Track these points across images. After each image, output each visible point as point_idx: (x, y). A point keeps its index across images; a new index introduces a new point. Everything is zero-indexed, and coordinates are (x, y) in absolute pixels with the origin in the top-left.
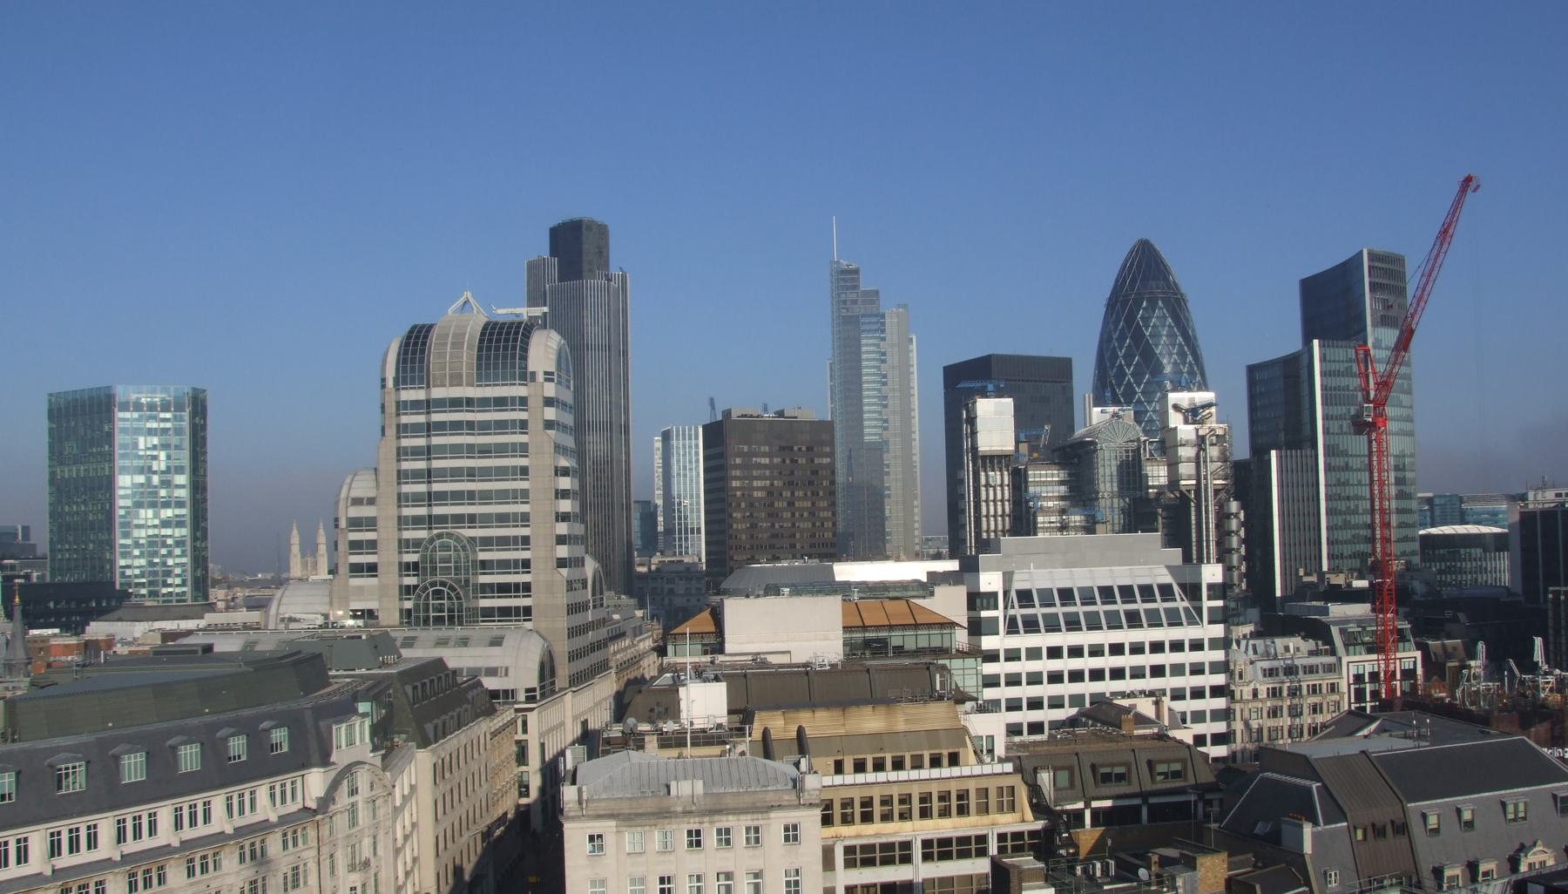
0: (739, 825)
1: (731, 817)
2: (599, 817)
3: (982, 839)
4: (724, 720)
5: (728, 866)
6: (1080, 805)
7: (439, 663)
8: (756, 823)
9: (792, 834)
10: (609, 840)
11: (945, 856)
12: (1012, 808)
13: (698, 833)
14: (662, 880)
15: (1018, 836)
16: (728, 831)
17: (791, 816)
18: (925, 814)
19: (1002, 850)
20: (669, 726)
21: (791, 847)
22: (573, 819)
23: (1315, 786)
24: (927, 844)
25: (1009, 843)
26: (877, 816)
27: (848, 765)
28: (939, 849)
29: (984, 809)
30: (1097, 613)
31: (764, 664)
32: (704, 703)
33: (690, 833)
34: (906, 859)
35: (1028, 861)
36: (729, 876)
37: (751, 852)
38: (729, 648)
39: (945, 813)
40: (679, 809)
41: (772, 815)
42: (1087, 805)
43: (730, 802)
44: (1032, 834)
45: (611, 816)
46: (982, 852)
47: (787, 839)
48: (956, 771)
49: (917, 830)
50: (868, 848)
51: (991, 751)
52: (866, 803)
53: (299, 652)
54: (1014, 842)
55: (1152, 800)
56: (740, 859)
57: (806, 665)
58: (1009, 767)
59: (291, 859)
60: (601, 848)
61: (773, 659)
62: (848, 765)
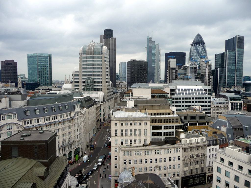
0: (138, 122)
1: (137, 121)
2: (117, 120)
3: (173, 126)
4: (134, 107)
6: (188, 122)
7: (89, 96)
8: (140, 122)
9: (146, 124)
10: (118, 124)
11: (167, 129)
13: (132, 123)
15: (178, 126)
16: (136, 123)
17: (146, 122)
18: (164, 122)
19: (176, 128)
20: (126, 107)
21: (145, 126)
22: (112, 121)
23: (227, 121)
24: (164, 127)
25: (177, 127)
26: (157, 122)
27: (153, 114)
28: (166, 128)
29: (173, 122)
30: (200, 93)
31: (139, 98)
32: (131, 104)
33: (130, 123)
34: (161, 129)
35: (181, 130)
36: (136, 130)
37: (140, 127)
38: (134, 96)
39: (167, 122)
40: (129, 120)
41: (143, 121)
42: (189, 122)
43: (137, 119)
44: (181, 126)
45: (119, 120)
46: (173, 128)
47: (145, 125)
48: (169, 116)
49: (163, 125)
50: (155, 127)
51: (174, 113)
52: (161, 120)
53: (69, 94)
54: (178, 127)
55: (199, 122)
56: (137, 127)
57: (146, 99)
58: (178, 116)
59: (69, 125)
60: (117, 125)
61: (140, 98)
62: (153, 114)
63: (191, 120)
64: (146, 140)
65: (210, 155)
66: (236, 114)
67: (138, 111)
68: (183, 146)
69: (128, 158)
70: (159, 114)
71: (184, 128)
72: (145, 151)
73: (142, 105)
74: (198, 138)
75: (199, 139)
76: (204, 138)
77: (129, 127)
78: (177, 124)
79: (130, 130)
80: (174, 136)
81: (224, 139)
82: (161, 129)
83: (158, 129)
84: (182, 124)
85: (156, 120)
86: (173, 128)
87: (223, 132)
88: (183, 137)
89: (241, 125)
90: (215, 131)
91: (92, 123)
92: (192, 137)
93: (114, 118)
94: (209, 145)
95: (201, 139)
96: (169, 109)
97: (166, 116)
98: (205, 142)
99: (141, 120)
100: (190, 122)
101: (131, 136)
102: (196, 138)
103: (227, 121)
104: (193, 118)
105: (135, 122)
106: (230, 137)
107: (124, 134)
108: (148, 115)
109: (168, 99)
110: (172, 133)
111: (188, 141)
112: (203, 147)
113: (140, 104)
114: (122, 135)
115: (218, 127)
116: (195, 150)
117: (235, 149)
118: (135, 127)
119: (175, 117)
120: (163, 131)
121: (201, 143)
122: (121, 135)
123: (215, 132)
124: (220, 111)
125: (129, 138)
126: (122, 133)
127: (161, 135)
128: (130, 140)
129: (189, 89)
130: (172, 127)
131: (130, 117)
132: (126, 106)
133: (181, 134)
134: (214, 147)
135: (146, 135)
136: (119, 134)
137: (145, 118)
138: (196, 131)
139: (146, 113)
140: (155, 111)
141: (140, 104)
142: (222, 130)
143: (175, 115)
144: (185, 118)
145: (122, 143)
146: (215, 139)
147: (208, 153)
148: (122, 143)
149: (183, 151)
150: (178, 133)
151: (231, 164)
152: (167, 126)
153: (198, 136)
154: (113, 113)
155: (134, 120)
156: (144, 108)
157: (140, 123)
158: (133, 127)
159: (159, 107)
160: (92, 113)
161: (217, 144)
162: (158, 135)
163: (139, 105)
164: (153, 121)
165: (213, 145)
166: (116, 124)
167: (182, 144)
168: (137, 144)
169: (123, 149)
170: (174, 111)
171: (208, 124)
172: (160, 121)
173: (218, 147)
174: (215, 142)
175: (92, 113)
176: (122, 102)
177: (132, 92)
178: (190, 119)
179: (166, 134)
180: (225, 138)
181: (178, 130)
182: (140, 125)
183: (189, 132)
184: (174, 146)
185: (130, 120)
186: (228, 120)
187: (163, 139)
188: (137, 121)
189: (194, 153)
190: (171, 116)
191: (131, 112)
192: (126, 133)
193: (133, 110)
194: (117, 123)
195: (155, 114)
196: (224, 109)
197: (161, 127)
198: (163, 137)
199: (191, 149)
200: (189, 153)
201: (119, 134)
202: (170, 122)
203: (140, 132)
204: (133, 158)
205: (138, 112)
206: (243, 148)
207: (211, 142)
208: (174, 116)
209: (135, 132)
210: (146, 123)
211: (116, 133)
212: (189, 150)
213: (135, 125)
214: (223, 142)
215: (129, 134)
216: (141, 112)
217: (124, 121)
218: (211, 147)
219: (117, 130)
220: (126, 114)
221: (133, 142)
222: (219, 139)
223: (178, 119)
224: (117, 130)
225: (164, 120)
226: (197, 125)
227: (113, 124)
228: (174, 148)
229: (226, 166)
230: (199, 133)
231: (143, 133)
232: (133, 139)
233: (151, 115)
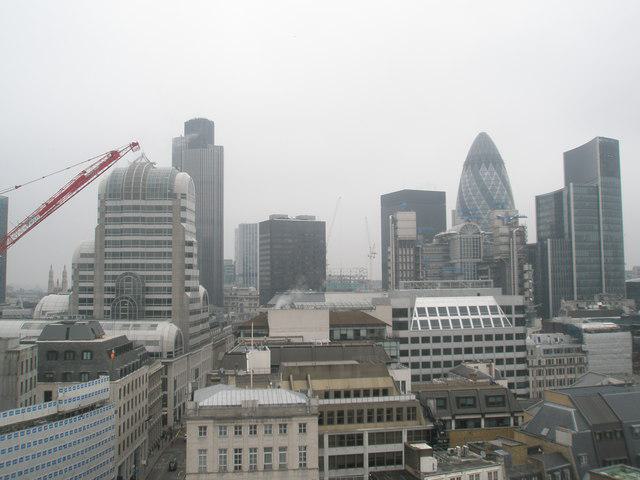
0: (276, 424)
9: (303, 429)
10: (210, 429)
12: (414, 418)
14: (236, 451)
17: (303, 420)
18: (370, 420)
20: (241, 373)
22: (188, 419)
26: (346, 420)
27: (332, 394)
29: (399, 419)
31: (289, 342)
32: (259, 360)
34: (360, 443)
35: (425, 446)
38: (271, 334)
40: (246, 415)
41: (294, 419)
42: (453, 417)
43: (273, 412)
45: (211, 418)
47: (300, 431)
48: (386, 399)
49: (365, 429)
50: (342, 437)
51: (404, 388)
54: (415, 436)
56: (276, 440)
57: (311, 343)
60: (205, 434)
62: (332, 394)
66: (602, 386)
67: (277, 384)
70: (342, 394)
71: (436, 438)
73: (291, 364)
74: (479, 471)
77: (246, 441)
78: (413, 426)
82: (360, 443)
84: (430, 426)
85: (331, 414)
87: (560, 449)
88: (430, 470)
90: (537, 444)
91: (132, 429)
92: (461, 466)
95: (490, 474)
97: (376, 399)
100: (457, 417)
103: (572, 411)
105: (269, 422)
106: (584, 462)
107: (231, 465)
110: (394, 458)
115: (545, 432)
118: (266, 438)
119: (405, 402)
123: (536, 448)
126: (223, 460)
127: (361, 465)
129: (424, 309)
130: (394, 437)
132: (245, 368)
133: (422, 458)
135: (305, 465)
138: (472, 448)
139: (306, 392)
140: (338, 384)
141: (290, 359)
142: (558, 440)
143: (408, 397)
144: (443, 403)
150: (413, 457)
156: (302, 374)
157: (285, 426)
158: (261, 441)
159: (353, 372)
160: (131, 396)
162: (351, 466)
163: (286, 364)
164: (325, 417)
166: (203, 430)
170: (404, 382)
171: (516, 424)
175: (131, 396)
176: (233, 354)
177: (266, 317)
179: (376, 459)
181: (413, 446)
185: (251, 417)
186: (576, 407)
188: (273, 417)
190: (391, 398)
191: (254, 387)
193: (261, 381)
194: (205, 428)
195: (337, 395)
196: (561, 372)
197: (360, 436)
202: (389, 419)
203: (283, 457)
205: (279, 387)
208: (402, 398)
209: (268, 458)
210: (305, 425)
211: (203, 460)
216: (291, 389)
219: (205, 451)
220: (238, 396)
222: (548, 472)
223: (414, 409)
224: (205, 451)
225: (370, 412)
226: (480, 426)
227: (192, 430)
230: (483, 454)
231: (293, 461)
233: (327, 395)
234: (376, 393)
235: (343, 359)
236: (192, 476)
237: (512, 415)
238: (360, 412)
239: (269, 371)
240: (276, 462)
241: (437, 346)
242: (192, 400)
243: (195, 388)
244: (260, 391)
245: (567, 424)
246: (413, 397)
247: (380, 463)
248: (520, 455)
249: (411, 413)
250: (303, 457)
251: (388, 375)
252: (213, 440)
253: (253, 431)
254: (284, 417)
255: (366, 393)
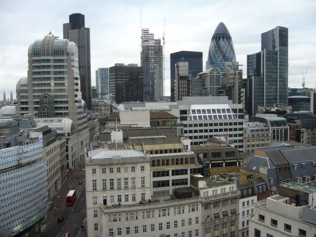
2: (95, 165)
3: (186, 170)
5: (126, 177)
9: (143, 169)
10: (98, 170)
11: (177, 174)
12: (194, 163)
17: (143, 165)
20: (109, 142)
22: (87, 166)
24: (173, 171)
27: (154, 152)
28: (175, 173)
29: (186, 163)
31: (130, 127)
32: (117, 136)
33: (117, 168)
34: (168, 175)
36: (127, 179)
37: (133, 173)
38: (121, 123)
39: (177, 164)
42: (210, 162)
43: (128, 161)
44: (199, 169)
46: (186, 173)
47: (141, 170)
48: (180, 154)
49: (170, 168)
51: (187, 149)
53: (12, 124)
54: (194, 171)
55: (226, 161)
56: (130, 174)
57: (142, 127)
58: (193, 153)
61: (133, 126)
62: (154, 152)
63: (214, 159)
64: (144, 194)
65: (244, 212)
66: (280, 147)
68: (203, 200)
69: (115, 226)
72: (144, 213)
73: (135, 138)
74: (225, 187)
75: (227, 188)
76: (234, 186)
77: (115, 176)
78: (193, 166)
79: (118, 180)
80: (189, 185)
81: (264, 186)
82: (168, 175)
83: (163, 175)
84: (201, 166)
86: (186, 173)
87: (262, 176)
88: (202, 187)
89: (286, 162)
91: (53, 171)
92: (217, 185)
93: (90, 161)
94: (243, 197)
96: (180, 142)
97: (175, 154)
98: (236, 192)
99: (135, 162)
100: (212, 162)
101: (119, 188)
102: (223, 187)
103: (268, 158)
104: (217, 155)
106: (272, 182)
107: (108, 186)
108: (146, 153)
109: (177, 126)
110: (184, 182)
111: (210, 192)
112: (234, 199)
113: (131, 135)
114: (105, 189)
116: (221, 205)
117: (280, 200)
120: (171, 178)
121: (230, 194)
122: (103, 189)
123: (251, 175)
124: (257, 143)
125: (116, 193)
126: (105, 185)
127: (168, 185)
128: (118, 196)
130: (184, 172)
131: (117, 158)
132: (110, 140)
134: (250, 199)
136: (100, 186)
137: (142, 159)
138: (221, 176)
139: (143, 151)
141: (131, 135)
142: (261, 172)
143: (190, 153)
144: (205, 155)
145: (105, 202)
146: (250, 186)
147: (241, 209)
148: (105, 202)
149: (204, 207)
150: (194, 181)
151: (274, 222)
152: (177, 171)
153: (225, 184)
154: (89, 153)
155: (124, 162)
156: (139, 143)
157: (134, 167)
159: (164, 141)
160: (52, 155)
161: (253, 194)
164: (153, 163)
165: (248, 196)
166: (94, 171)
167: (202, 198)
168: (130, 202)
169: (106, 211)
170: (187, 146)
171: (239, 164)
172: (166, 162)
173: (255, 198)
174: (250, 190)
175: (52, 155)
178: (213, 158)
179: (175, 183)
180: (266, 184)
182: (134, 170)
183: (212, 178)
184: (188, 201)
185: (117, 164)
187: (171, 191)
189: (220, 210)
190: (183, 154)
192: (112, 184)
193: (120, 147)
194: (95, 170)
195: (157, 152)
197: (168, 172)
198: (171, 188)
199: (216, 203)
200: (213, 211)
201: (100, 186)
202: (182, 163)
203: (134, 183)
204: (124, 224)
206: (291, 198)
207: (245, 191)
208: (188, 153)
209: (126, 183)
210: (144, 167)
211: (95, 185)
212: (212, 206)
213: (126, 171)
214: (262, 191)
215: (115, 186)
217: (107, 165)
218: (245, 200)
219: (96, 181)
221: (123, 198)
227: (88, 171)
228: (189, 204)
229: (268, 227)
231: (138, 184)
232: (123, 193)
233: (151, 153)
234: (175, 151)
235: (158, 135)
236: (90, 193)
237: (238, 161)
238: (168, 160)
239: (122, 141)
240: (130, 185)
241: (221, 127)
242: (88, 156)
243: (88, 151)
244: (121, 151)
245: (265, 165)
246: (193, 153)
247: (177, 184)
248: (243, 179)
249: (192, 160)
250: (143, 182)
251: (181, 143)
252: (99, 176)
253: (119, 170)
254: (134, 163)
255: (171, 151)
